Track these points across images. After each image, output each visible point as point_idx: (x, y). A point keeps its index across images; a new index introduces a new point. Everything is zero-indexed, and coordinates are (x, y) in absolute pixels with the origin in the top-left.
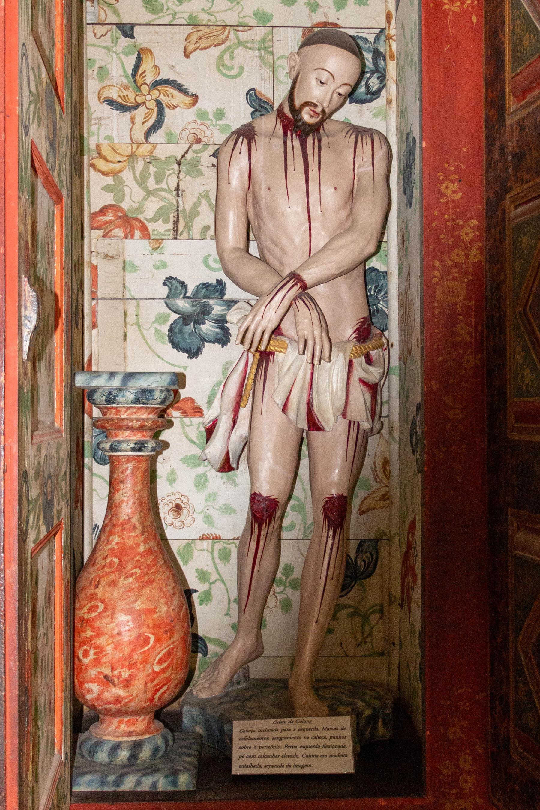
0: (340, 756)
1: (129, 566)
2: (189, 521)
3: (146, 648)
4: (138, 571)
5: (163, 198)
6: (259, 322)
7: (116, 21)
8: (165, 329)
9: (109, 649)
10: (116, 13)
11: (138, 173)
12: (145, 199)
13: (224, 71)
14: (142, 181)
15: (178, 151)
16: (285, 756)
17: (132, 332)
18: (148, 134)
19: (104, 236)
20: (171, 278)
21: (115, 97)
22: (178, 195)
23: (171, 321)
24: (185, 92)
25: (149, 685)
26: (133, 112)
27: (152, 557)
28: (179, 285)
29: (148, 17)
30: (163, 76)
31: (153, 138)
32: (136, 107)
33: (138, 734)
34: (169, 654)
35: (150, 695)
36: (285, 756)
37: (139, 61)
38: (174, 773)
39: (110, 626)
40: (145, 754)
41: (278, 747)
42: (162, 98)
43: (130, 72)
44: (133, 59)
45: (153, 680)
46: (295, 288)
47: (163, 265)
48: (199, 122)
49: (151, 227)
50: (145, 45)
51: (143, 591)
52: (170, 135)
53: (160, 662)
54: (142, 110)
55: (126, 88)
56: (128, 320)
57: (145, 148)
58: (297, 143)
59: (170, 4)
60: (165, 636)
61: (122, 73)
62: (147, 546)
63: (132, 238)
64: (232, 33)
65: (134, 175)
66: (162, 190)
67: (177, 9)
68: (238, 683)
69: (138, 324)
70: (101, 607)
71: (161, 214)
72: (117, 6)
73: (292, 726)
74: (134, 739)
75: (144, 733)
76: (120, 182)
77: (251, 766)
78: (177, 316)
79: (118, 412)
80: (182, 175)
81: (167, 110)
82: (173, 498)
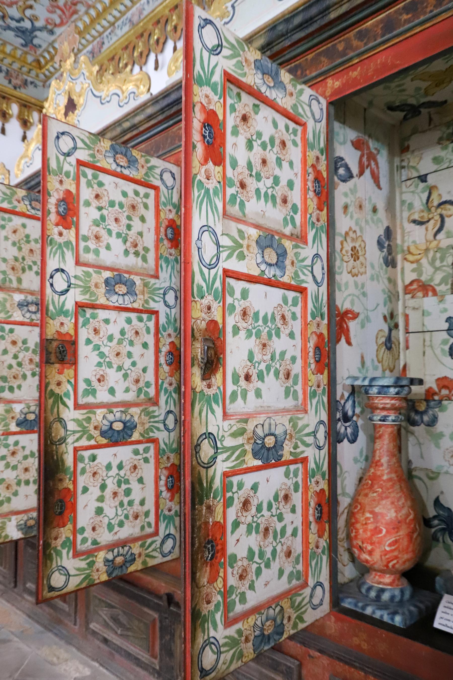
1: (376, 486)
3: (380, 535)
4: (380, 490)
5: (444, 271)
8: (447, 348)
10: (417, 171)
11: (430, 259)
12: (434, 273)
14: (432, 263)
25: (383, 557)
27: (391, 483)
29: (435, 167)
30: (444, 199)
32: (428, 221)
33: (384, 584)
34: (396, 542)
35: (385, 563)
40: (386, 596)
43: (425, 201)
44: (426, 194)
45: (385, 555)
47: (445, 310)
49: (438, 289)
50: (433, 184)
51: (381, 502)
53: (390, 545)
54: (432, 222)
55: (423, 211)
56: (426, 343)
57: (434, 243)
60: (393, 531)
61: (420, 203)
62: (389, 476)
66: (444, 266)
69: (431, 346)
71: (443, 281)
72: (418, 167)
74: (381, 586)
79: (373, 399)
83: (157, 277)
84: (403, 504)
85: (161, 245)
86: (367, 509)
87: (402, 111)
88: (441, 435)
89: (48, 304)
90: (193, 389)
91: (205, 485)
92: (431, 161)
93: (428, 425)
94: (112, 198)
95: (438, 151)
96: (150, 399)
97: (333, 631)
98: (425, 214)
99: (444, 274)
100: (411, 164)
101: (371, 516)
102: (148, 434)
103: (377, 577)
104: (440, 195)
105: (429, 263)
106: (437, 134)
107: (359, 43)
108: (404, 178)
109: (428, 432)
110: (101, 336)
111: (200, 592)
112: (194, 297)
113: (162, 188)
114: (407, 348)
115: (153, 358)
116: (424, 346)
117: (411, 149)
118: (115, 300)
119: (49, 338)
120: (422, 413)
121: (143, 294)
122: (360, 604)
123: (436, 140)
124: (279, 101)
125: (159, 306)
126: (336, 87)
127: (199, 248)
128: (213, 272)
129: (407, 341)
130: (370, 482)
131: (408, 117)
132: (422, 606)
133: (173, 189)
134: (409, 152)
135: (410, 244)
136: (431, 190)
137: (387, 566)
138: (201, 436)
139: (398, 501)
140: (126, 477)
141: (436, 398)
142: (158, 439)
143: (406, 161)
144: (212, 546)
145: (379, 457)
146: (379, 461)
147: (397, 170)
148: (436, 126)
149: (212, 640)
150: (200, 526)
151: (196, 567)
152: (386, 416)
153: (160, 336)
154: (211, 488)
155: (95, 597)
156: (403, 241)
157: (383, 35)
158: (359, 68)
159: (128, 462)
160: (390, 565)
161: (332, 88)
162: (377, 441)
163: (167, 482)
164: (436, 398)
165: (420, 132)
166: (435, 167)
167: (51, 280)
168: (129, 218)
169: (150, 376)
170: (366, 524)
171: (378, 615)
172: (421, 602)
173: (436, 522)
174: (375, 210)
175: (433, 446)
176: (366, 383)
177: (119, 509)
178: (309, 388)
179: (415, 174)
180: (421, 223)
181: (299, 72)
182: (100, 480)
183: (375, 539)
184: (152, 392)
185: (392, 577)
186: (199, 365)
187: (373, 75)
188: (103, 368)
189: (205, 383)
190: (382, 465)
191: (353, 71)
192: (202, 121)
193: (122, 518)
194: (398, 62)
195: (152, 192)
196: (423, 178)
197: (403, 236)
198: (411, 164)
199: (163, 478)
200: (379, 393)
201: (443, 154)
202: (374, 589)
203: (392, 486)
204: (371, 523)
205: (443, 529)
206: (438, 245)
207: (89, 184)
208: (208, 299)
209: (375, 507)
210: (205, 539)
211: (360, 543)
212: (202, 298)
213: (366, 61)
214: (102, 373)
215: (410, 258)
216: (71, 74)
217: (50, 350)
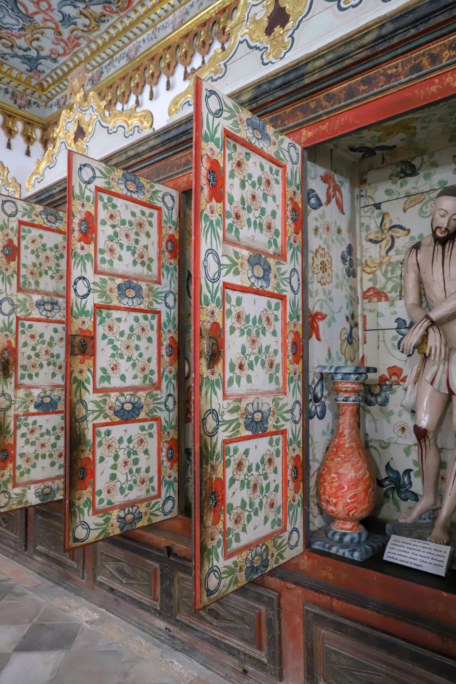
1: (340, 453)
4: (343, 455)
5: (395, 281)
8: (396, 343)
10: (373, 200)
11: (383, 271)
12: (387, 282)
14: (385, 274)
15: (401, 258)
17: (381, 344)
18: (387, 252)
20: (399, 318)
22: (401, 279)
25: (345, 508)
26: (381, 243)
27: (351, 450)
28: (402, 322)
29: (387, 198)
30: (394, 224)
31: (390, 254)
32: (382, 241)
33: (346, 529)
34: (355, 496)
35: (346, 513)
37: (383, 219)
38: (354, 551)
40: (347, 539)
43: (379, 225)
44: (380, 219)
45: (347, 506)
49: (389, 295)
50: (386, 211)
53: (350, 498)
54: (385, 241)
55: (377, 233)
56: (380, 339)
57: (387, 258)
60: (353, 487)
61: (375, 226)
62: (350, 445)
65: (382, 272)
66: (394, 277)
67: (400, 191)
69: (384, 341)
71: (394, 289)
74: (343, 531)
75: (349, 530)
79: (338, 384)
83: (159, 283)
84: (361, 466)
85: (162, 256)
86: (333, 470)
87: (361, 152)
88: (392, 413)
89: (72, 306)
90: (201, 376)
91: (210, 449)
92: (384, 192)
93: (381, 405)
94: (123, 218)
95: (389, 185)
96: (154, 384)
97: (306, 567)
98: (380, 235)
99: (394, 284)
100: (368, 194)
101: (336, 476)
102: (152, 414)
103: (340, 524)
104: (391, 220)
105: (383, 275)
106: (388, 171)
107: (327, 104)
108: (362, 205)
109: (381, 410)
110: (114, 332)
111: (206, 531)
112: (202, 305)
113: (164, 209)
114: (365, 342)
115: (156, 350)
116: (378, 341)
117: (368, 181)
118: (126, 303)
119: (73, 334)
120: (377, 395)
121: (148, 297)
122: (327, 546)
123: (388, 176)
124: (265, 149)
125: (161, 307)
126: (310, 136)
127: (205, 267)
128: (216, 285)
129: (365, 337)
130: (335, 449)
131: (366, 156)
132: (374, 545)
133: (172, 209)
134: (367, 184)
135: (367, 258)
136: (384, 216)
137: (348, 515)
138: (207, 411)
139: (357, 464)
140: (134, 449)
141: (388, 383)
142: (160, 417)
143: (364, 191)
144: (215, 497)
146: (342, 433)
147: (357, 198)
148: (387, 165)
149: (215, 568)
150: (206, 480)
151: (203, 512)
152: (347, 397)
153: (162, 332)
154: (214, 452)
155: (102, 553)
156: (362, 256)
157: (346, 100)
158: (327, 123)
159: (136, 437)
160: (351, 513)
161: (306, 137)
162: (341, 417)
163: (167, 453)
164: (388, 383)
165: (376, 169)
166: (387, 198)
167: (75, 286)
168: (137, 234)
169: (154, 366)
170: (332, 482)
171: (341, 553)
172: (374, 542)
173: (387, 482)
174: (339, 231)
175: (385, 421)
176: (333, 371)
177: (129, 476)
178: (288, 375)
179: (372, 203)
180: (376, 242)
181: (279, 122)
182: (114, 452)
183: (339, 494)
184: (155, 378)
185: (352, 524)
186: (205, 357)
187: (338, 130)
188: (116, 358)
189: (209, 371)
191: (322, 125)
192: (208, 168)
193: (132, 482)
194: (358, 122)
195: (155, 212)
196: (378, 205)
197: (362, 252)
198: (368, 194)
199: (165, 450)
200: (343, 379)
201: (393, 187)
202: (338, 533)
203: (352, 452)
204: (336, 481)
205: (393, 488)
206: (389, 260)
207: (105, 207)
208: (213, 306)
209: (339, 469)
210: (210, 491)
211: (327, 498)
212: (208, 305)
213: (332, 118)
214: (115, 363)
215: (368, 269)
216: (80, 106)
217: (74, 344)
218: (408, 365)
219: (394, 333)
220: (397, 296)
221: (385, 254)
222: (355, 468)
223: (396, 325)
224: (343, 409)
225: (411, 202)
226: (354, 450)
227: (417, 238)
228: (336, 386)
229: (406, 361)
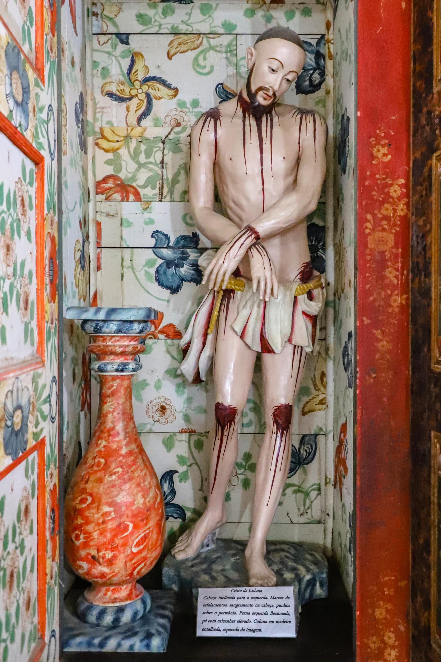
0: (284, 622)
1: (113, 466)
2: (170, 419)
3: (126, 534)
4: (120, 470)
5: (151, 170)
6: (221, 267)
7: (115, 31)
8: (153, 271)
9: (95, 535)
10: (115, 25)
11: (132, 150)
12: (138, 170)
13: (198, 69)
14: (135, 156)
15: (162, 132)
16: (240, 621)
17: (128, 273)
18: (139, 120)
19: (106, 199)
20: (157, 231)
21: (114, 91)
23: (157, 265)
24: (168, 86)
25: (128, 564)
26: (128, 103)
27: (132, 458)
28: (163, 237)
29: (139, 28)
30: (151, 74)
31: (144, 123)
32: (130, 99)
33: (121, 600)
34: (145, 537)
35: (129, 571)
36: (240, 621)
38: (149, 636)
39: (97, 516)
40: (126, 617)
41: (235, 613)
42: (151, 91)
43: (126, 71)
45: (131, 560)
46: (250, 239)
47: (152, 222)
48: (179, 109)
51: (123, 487)
52: (156, 120)
53: (138, 545)
54: (135, 101)
55: (123, 84)
56: (124, 264)
57: (137, 131)
58: (253, 122)
59: (157, 18)
60: (141, 524)
62: (129, 449)
63: (128, 200)
64: (205, 39)
66: (151, 163)
67: (163, 21)
68: (208, 546)
70: (90, 499)
71: (149, 182)
72: (116, 19)
73: (246, 595)
74: (118, 604)
76: (118, 157)
77: (212, 629)
78: (162, 261)
79: (104, 340)
80: (166, 151)
81: (154, 101)
82: (159, 401)
84: (150, 483)
99: (150, 174)
100: (105, 13)
101: (112, 509)
103: (109, 593)
105: (130, 155)
108: (96, 30)
114: (99, 268)
129: (99, 259)
130: (102, 461)
135: (104, 125)
139: (144, 481)
143: (99, 5)
145: (113, 422)
146: (113, 428)
147: (88, 16)
152: (125, 365)
160: (135, 572)
162: (108, 400)
176: (101, 316)
178: (46, 324)
180: (121, 99)
183: (118, 541)
190: (118, 434)
196: (124, 37)
197: (95, 113)
200: (119, 331)
203: (134, 462)
204: (112, 519)
209: (117, 496)
215: (104, 144)
218: (171, 307)
219: (150, 254)
220: (155, 195)
221: (135, 123)
222: (142, 490)
223: (152, 242)
224: (112, 386)
225: (180, 44)
226: (136, 458)
227: (188, 106)
228: (100, 343)
229: (168, 301)
